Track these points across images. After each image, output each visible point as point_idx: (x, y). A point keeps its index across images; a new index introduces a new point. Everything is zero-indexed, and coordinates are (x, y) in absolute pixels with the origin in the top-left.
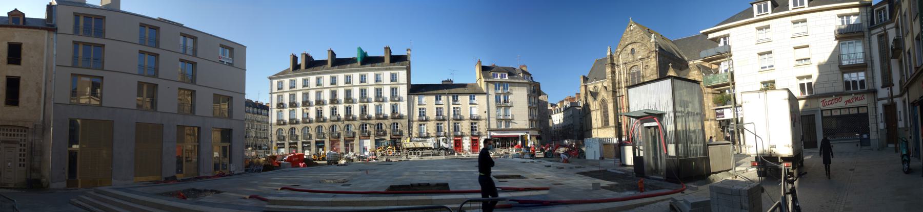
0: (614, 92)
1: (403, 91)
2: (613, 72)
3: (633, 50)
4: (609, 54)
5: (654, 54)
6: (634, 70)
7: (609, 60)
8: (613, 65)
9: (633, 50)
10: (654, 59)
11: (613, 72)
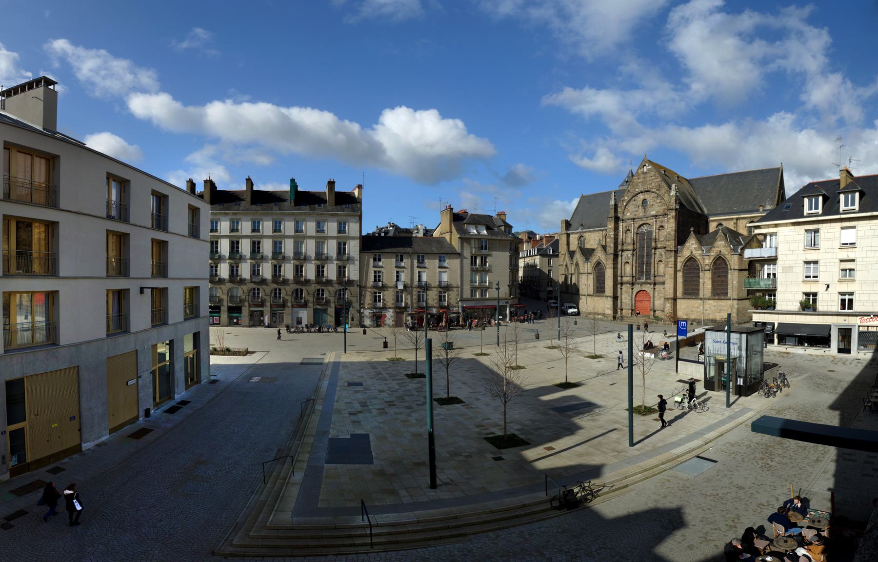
0: (616, 256)
1: (353, 248)
2: (616, 229)
3: (644, 201)
4: (612, 202)
5: (673, 213)
6: (644, 229)
7: (612, 213)
8: (617, 219)
9: (644, 201)
10: (672, 221)
11: (616, 229)
